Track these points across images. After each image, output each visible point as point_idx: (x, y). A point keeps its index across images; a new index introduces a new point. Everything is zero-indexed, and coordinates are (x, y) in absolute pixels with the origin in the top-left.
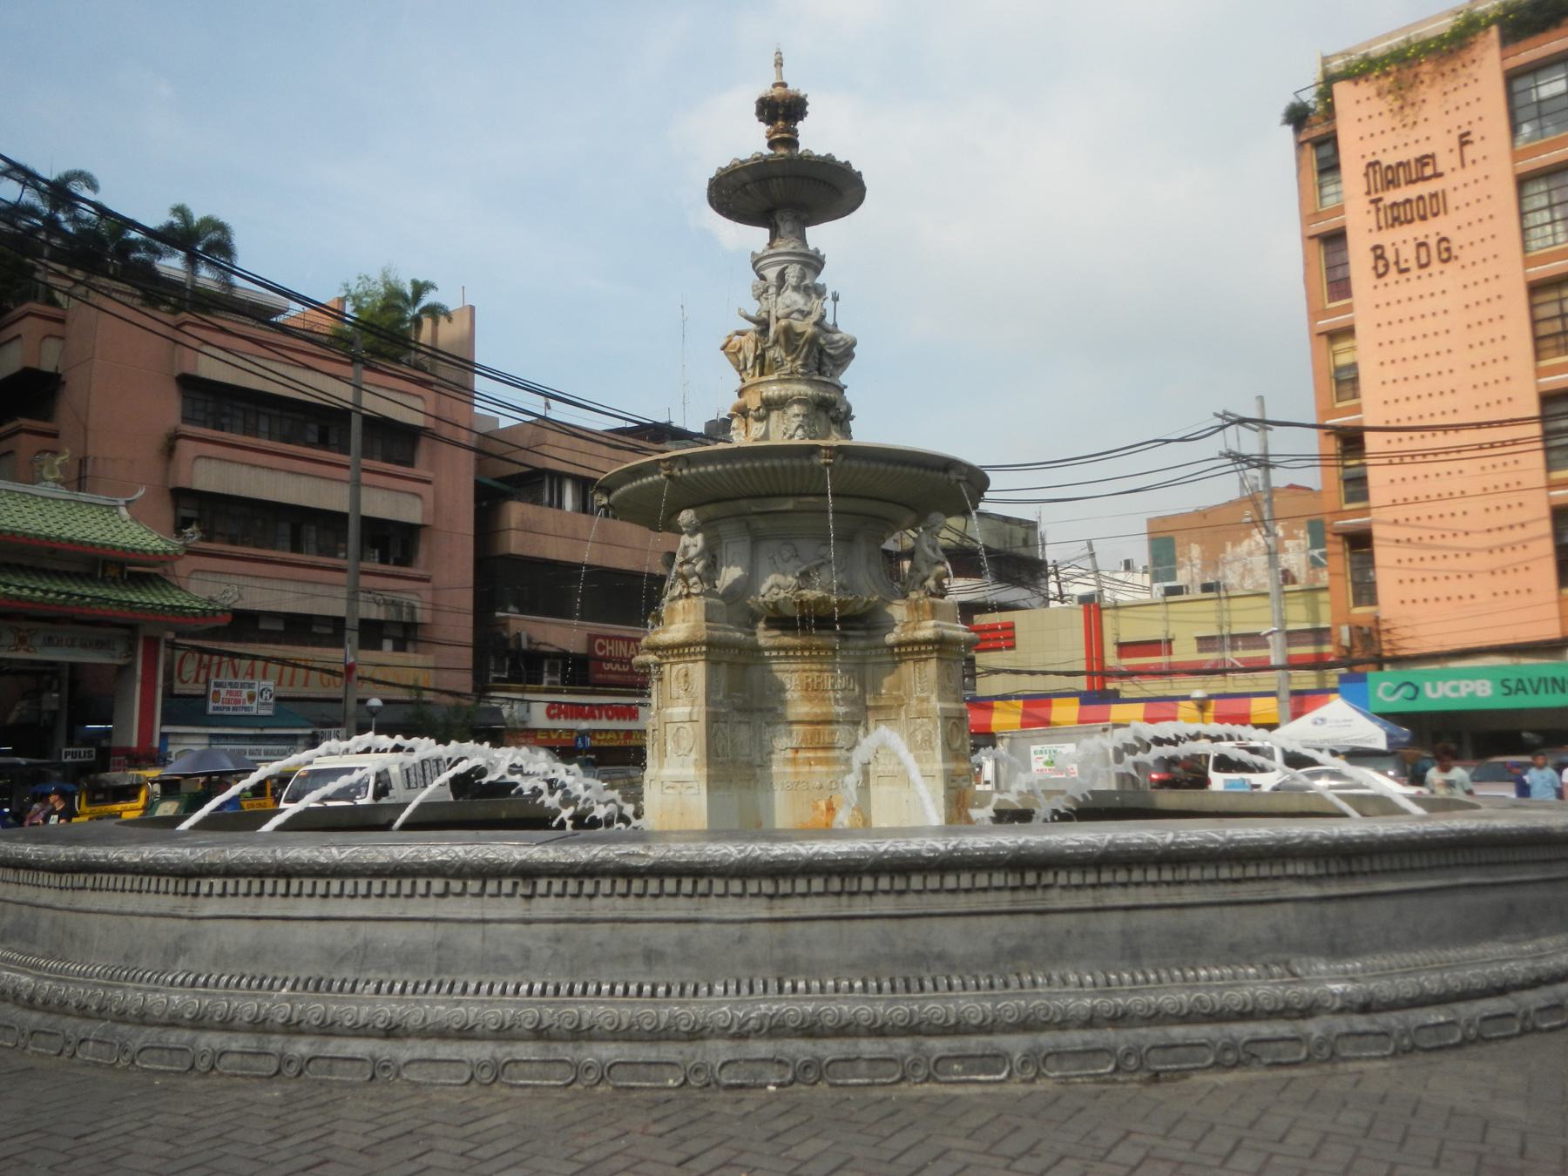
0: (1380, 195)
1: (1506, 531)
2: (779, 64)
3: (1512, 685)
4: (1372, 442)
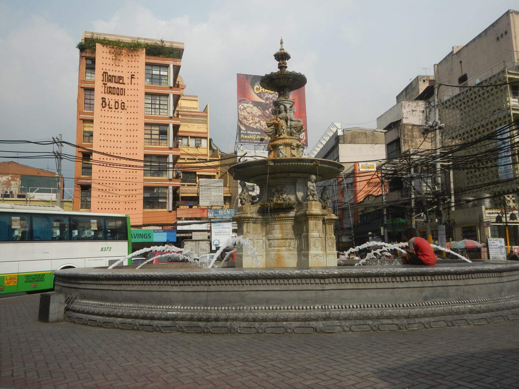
0: (106, 83)
1: (128, 191)
2: (282, 43)
4: (95, 156)
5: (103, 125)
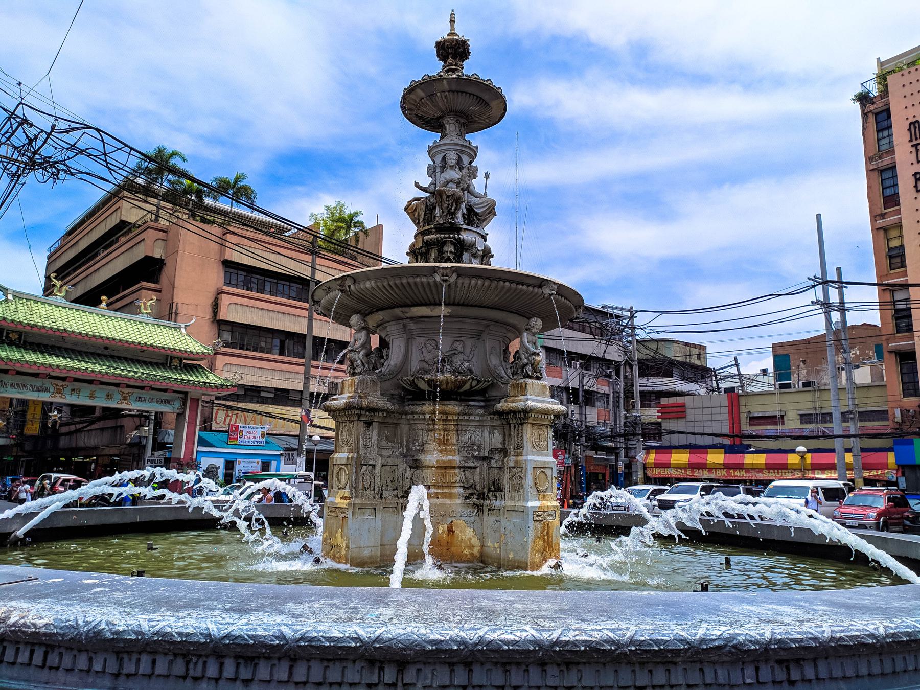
2: (452, 21)
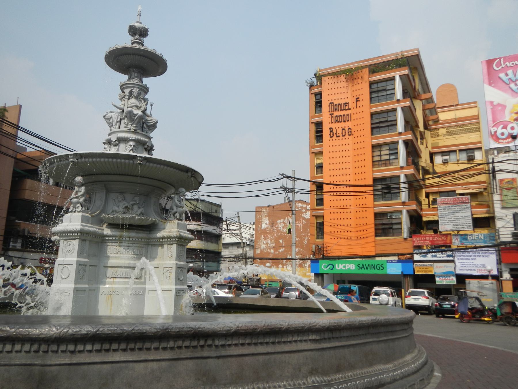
3: (361, 266)
4: (326, 188)
5: (332, 155)
